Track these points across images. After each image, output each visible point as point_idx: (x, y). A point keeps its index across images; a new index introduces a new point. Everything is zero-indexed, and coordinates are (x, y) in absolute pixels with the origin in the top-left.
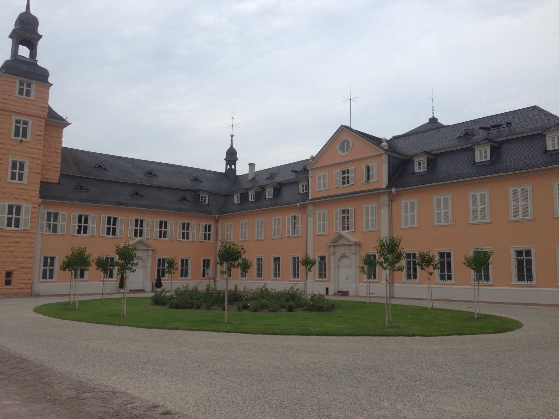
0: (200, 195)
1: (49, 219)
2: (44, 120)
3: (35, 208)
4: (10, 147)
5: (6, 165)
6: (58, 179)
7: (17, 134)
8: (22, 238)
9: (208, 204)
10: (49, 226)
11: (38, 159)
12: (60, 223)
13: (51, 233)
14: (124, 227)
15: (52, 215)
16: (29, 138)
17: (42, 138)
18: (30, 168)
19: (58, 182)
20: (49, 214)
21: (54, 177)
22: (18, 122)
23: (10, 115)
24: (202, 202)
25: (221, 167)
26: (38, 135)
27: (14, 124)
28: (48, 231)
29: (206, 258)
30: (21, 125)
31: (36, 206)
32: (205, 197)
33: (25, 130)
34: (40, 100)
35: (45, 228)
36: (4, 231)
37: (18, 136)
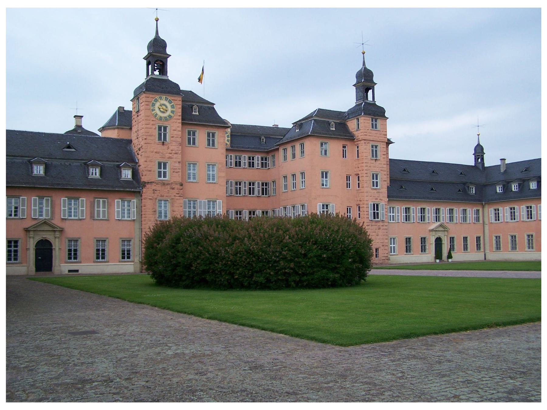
0: (470, 187)
7: (373, 156)
9: (475, 194)
16: (379, 158)
24: (471, 192)
25: (470, 161)
27: (371, 149)
29: (478, 235)
30: (374, 149)
32: (472, 188)
33: (376, 151)
34: (383, 130)
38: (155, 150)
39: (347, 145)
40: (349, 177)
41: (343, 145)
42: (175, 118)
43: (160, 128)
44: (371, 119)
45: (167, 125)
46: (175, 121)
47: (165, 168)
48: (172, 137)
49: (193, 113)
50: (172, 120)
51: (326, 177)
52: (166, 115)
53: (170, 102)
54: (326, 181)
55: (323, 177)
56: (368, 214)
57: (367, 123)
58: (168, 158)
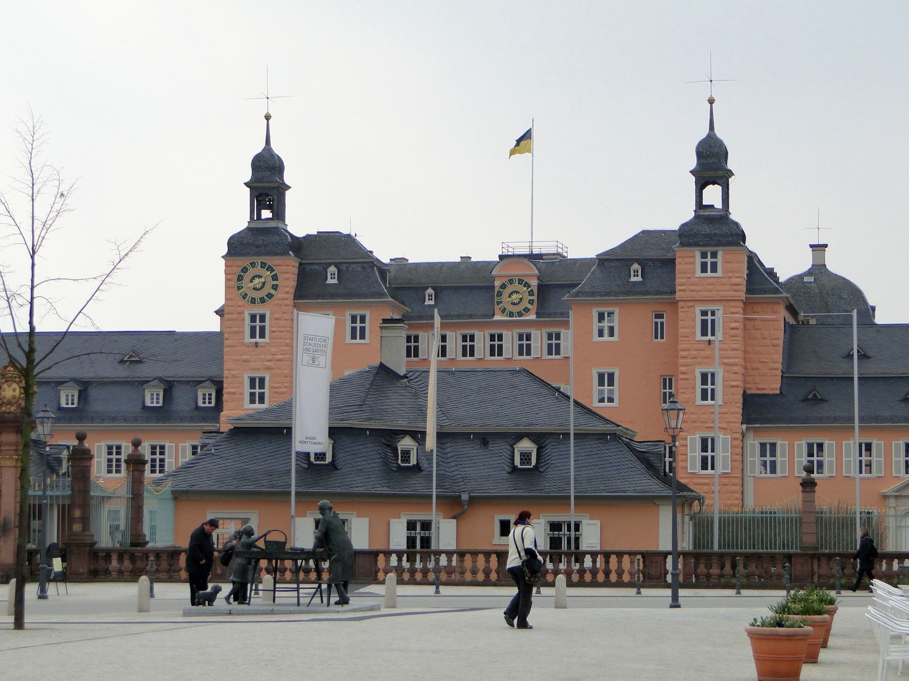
1: (763, 454)
2: (741, 305)
3: (736, 439)
4: (695, 352)
5: (693, 380)
6: (779, 388)
8: (722, 485)
10: (764, 464)
11: (736, 365)
12: (779, 459)
13: (769, 475)
14: (883, 459)
15: (768, 446)
16: (719, 335)
17: (740, 332)
18: (724, 380)
19: (778, 392)
20: (763, 445)
21: (771, 384)
22: (704, 313)
23: (691, 306)
26: (732, 329)
27: (699, 318)
28: (763, 472)
30: (709, 317)
31: (739, 436)
34: (730, 275)
35: (758, 467)
36: (697, 476)
37: (707, 335)
38: (244, 357)
39: (665, 311)
40: (670, 380)
41: (653, 312)
42: (279, 296)
43: (253, 318)
44: (698, 255)
45: (265, 312)
46: (280, 302)
47: (262, 386)
48: (273, 332)
49: (330, 281)
50: (274, 301)
51: (611, 383)
52: (263, 293)
53: (270, 269)
54: (611, 392)
55: (601, 383)
56: (686, 461)
57: (687, 263)
58: (264, 369)
